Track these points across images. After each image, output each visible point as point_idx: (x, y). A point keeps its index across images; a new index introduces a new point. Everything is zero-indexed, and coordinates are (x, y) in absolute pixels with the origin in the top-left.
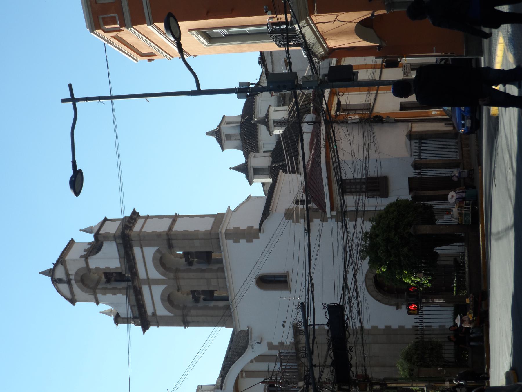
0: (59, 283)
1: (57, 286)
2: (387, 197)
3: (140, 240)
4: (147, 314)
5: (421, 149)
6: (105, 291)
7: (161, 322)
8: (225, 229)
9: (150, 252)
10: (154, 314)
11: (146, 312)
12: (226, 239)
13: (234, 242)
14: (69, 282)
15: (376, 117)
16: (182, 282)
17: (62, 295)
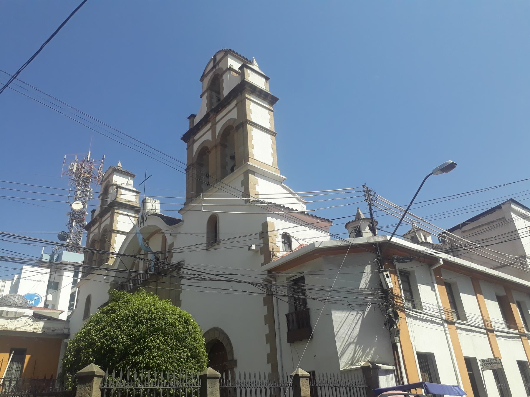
0: (213, 61)
1: (212, 60)
2: (288, 342)
3: (242, 102)
4: (194, 136)
5: (341, 388)
6: (210, 99)
7: (190, 148)
8: (254, 171)
9: (234, 115)
10: (194, 141)
11: (195, 134)
12: (244, 173)
13: (242, 181)
14: (214, 67)
15: (396, 316)
16: (213, 152)
17: (206, 68)
